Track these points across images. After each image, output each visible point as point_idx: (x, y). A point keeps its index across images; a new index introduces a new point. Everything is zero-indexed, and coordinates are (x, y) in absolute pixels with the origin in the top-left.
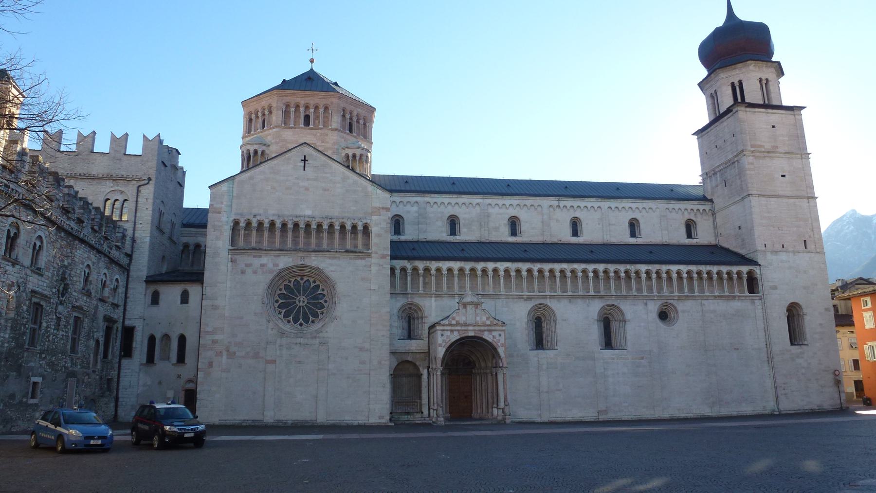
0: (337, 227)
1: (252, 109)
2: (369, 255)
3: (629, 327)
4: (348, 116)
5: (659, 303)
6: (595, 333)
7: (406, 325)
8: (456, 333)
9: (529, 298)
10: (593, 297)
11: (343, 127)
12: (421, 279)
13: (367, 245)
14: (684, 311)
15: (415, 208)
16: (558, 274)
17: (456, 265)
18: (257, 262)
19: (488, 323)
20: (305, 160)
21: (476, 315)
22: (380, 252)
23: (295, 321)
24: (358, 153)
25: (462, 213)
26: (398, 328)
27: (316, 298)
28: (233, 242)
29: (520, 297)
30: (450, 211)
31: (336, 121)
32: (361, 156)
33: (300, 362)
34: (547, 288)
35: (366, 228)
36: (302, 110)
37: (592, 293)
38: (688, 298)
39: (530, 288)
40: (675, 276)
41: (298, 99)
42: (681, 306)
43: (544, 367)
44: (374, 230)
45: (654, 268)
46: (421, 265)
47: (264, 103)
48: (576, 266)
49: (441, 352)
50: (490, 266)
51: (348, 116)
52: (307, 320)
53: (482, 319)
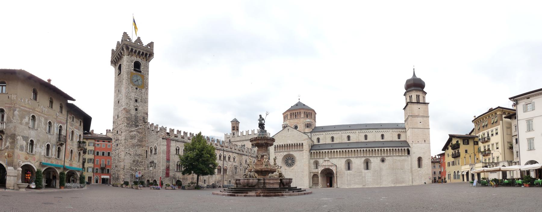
0: (296, 145)
1: (284, 115)
2: (303, 150)
3: (372, 164)
4: (306, 113)
5: (381, 158)
6: (363, 166)
7: (316, 166)
8: (323, 168)
9: (345, 158)
10: (362, 157)
11: (304, 116)
12: (318, 154)
13: (302, 148)
14: (387, 160)
15: (323, 135)
16: (353, 151)
17: (327, 151)
18: (279, 154)
19: (331, 165)
20: (288, 130)
21: (328, 163)
22: (305, 150)
23: (289, 166)
24: (308, 123)
25: (335, 136)
26: (313, 166)
27: (293, 161)
28: (275, 150)
29: (343, 158)
30: (332, 135)
31: (302, 115)
32: (309, 123)
33: (290, 175)
34: (350, 155)
35: (302, 144)
36: (294, 114)
37: (362, 156)
38: (389, 156)
39: (346, 155)
40: (385, 150)
41: (293, 112)
42: (387, 158)
43: (349, 175)
44: (304, 144)
45: (380, 149)
46: (318, 151)
47: (286, 114)
48: (358, 149)
49: (320, 172)
50: (335, 150)
51: (306, 113)
52: (291, 166)
53: (329, 164)
